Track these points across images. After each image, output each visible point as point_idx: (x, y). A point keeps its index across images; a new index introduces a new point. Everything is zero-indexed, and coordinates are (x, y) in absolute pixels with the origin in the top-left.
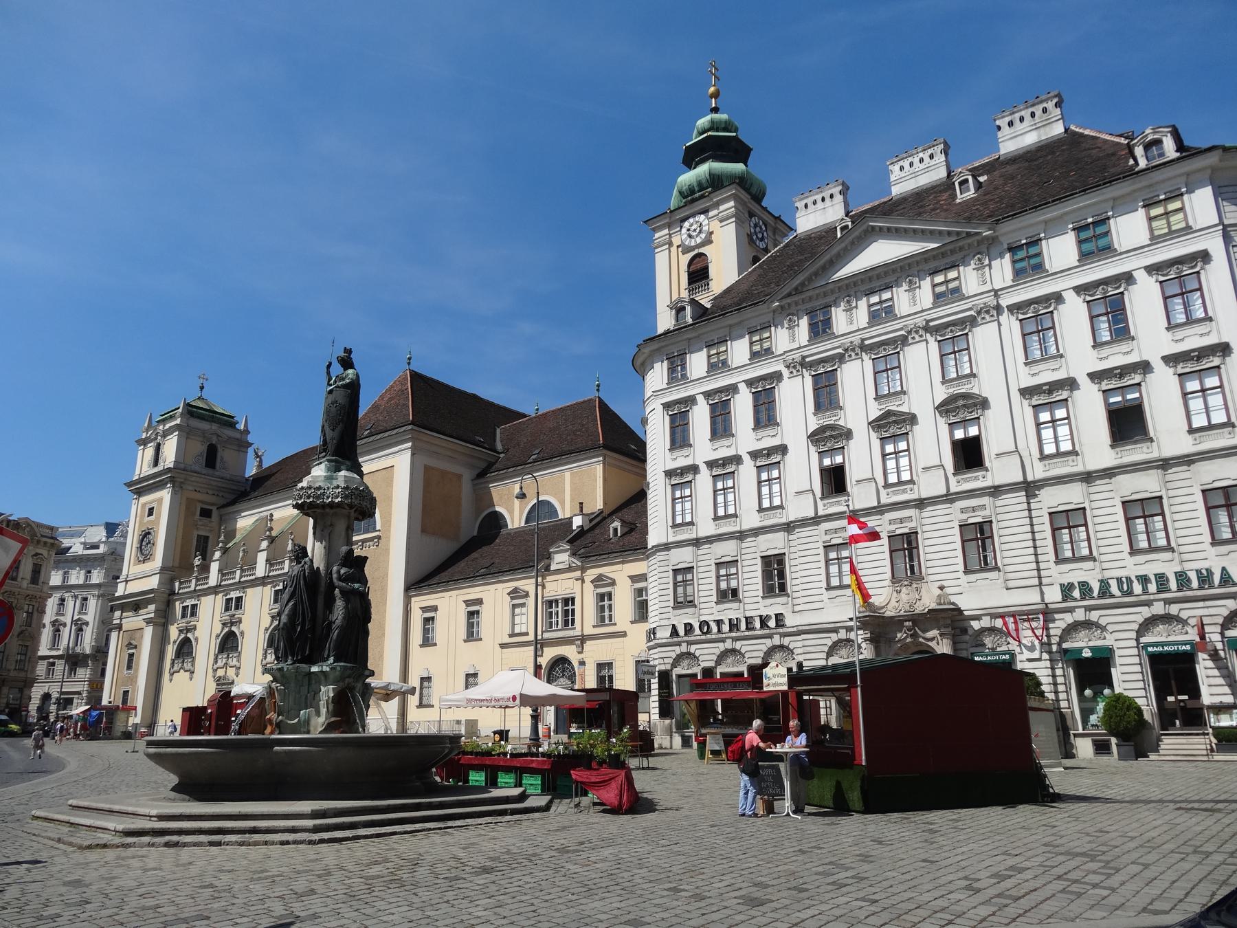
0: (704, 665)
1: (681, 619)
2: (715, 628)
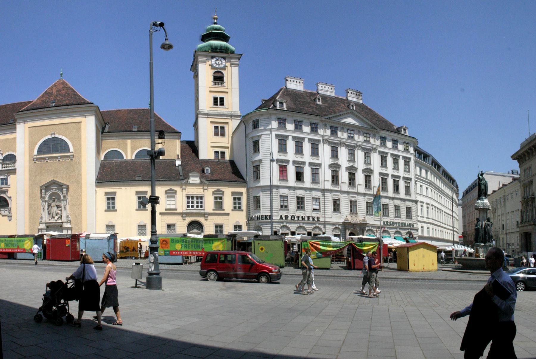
0: (292, 230)
1: (284, 213)
2: (296, 219)
